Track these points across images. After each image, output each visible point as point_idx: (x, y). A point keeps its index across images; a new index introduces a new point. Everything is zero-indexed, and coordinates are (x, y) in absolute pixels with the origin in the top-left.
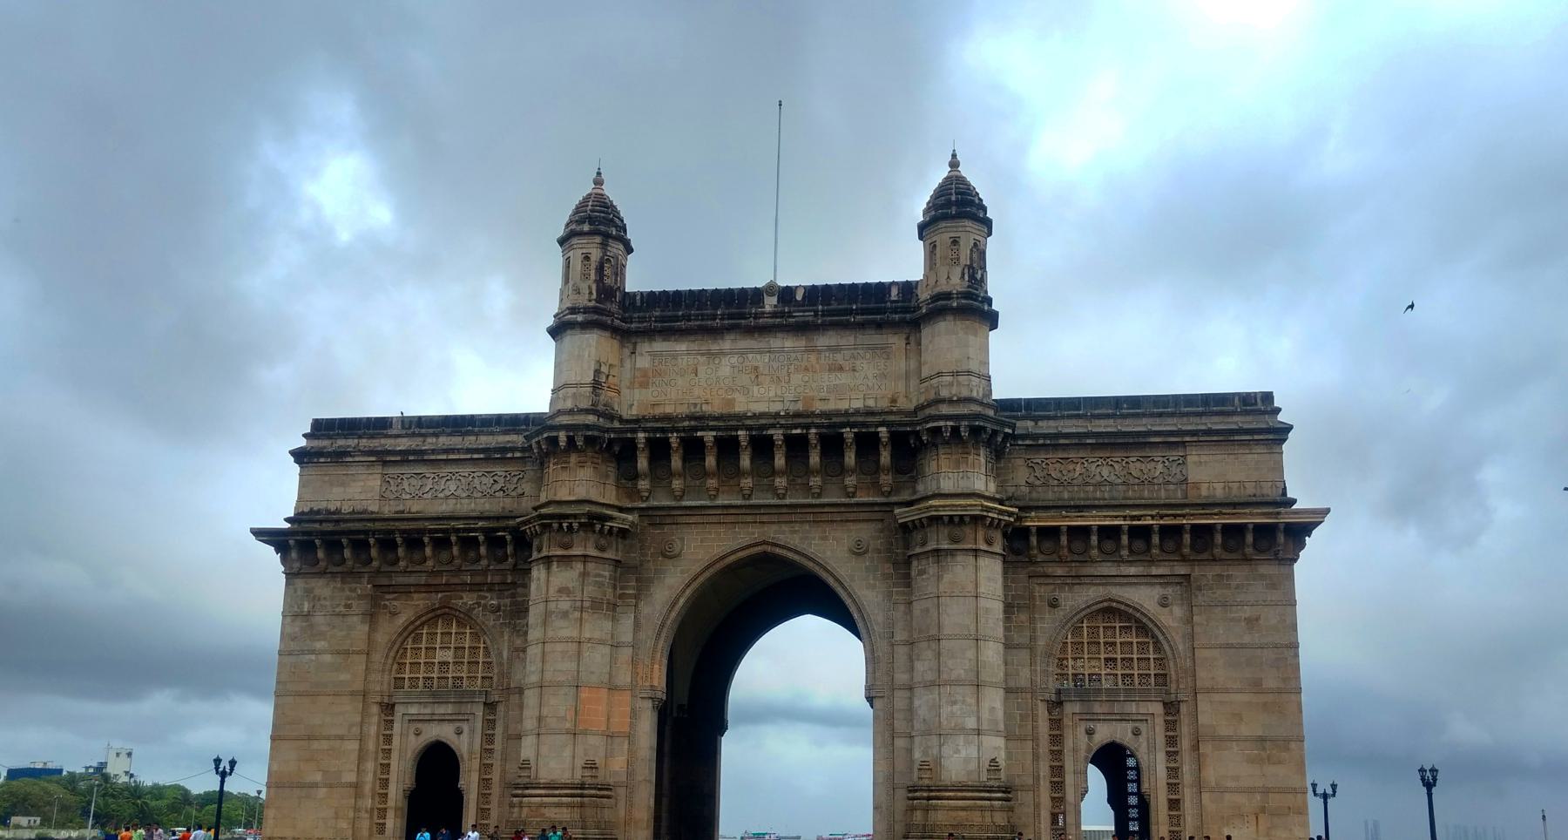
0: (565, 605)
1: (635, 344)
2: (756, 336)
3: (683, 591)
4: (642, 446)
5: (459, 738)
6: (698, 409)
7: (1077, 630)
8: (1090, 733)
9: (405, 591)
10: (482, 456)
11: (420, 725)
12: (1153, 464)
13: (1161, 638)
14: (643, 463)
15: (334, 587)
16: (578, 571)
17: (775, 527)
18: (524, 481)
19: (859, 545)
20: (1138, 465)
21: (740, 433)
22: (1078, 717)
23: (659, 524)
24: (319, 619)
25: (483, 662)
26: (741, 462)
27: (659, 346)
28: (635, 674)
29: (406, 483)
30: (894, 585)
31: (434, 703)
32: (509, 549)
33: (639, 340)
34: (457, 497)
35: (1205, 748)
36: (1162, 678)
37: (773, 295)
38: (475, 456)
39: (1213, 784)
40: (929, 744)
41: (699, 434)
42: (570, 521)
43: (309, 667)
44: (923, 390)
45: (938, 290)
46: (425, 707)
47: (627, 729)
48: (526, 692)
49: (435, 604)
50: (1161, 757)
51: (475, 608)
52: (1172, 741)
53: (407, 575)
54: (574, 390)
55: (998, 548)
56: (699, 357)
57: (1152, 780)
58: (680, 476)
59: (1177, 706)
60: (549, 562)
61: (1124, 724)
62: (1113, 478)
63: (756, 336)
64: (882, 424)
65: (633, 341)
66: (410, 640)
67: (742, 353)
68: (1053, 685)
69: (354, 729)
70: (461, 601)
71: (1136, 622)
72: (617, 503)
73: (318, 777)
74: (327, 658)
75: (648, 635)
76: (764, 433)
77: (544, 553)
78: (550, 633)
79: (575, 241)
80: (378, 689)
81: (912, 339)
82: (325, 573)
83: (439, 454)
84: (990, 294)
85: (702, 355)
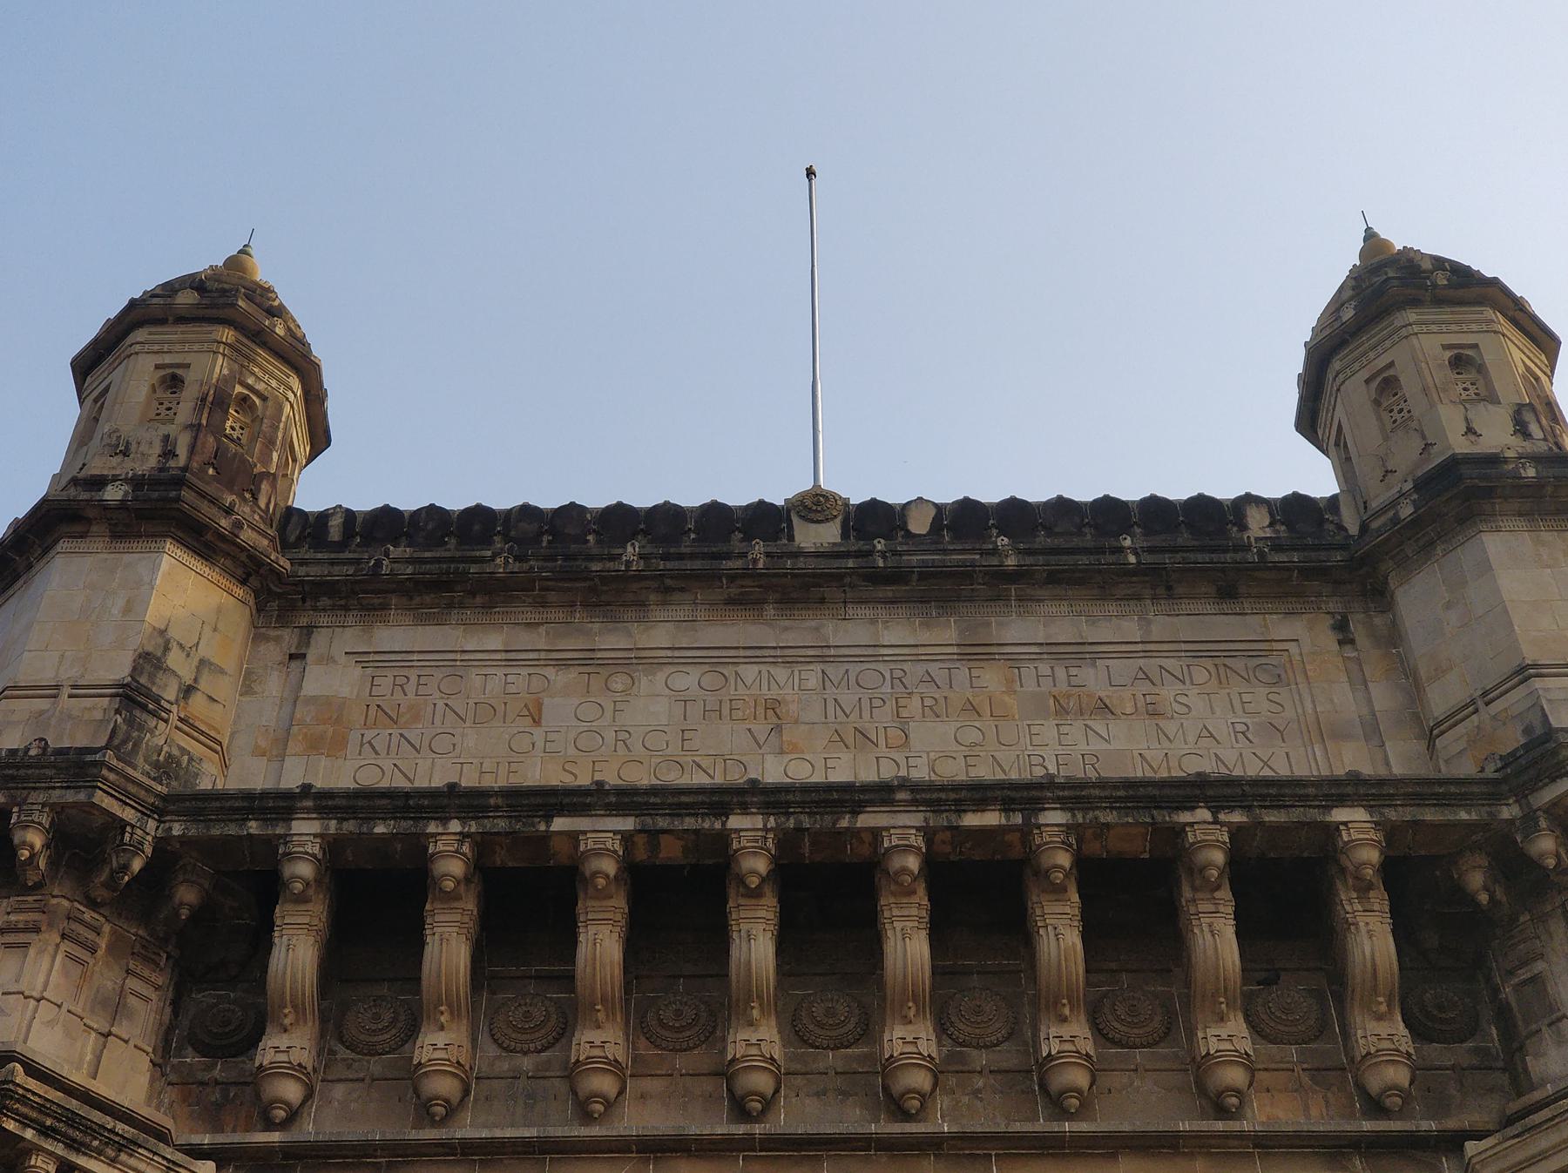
1: (309, 630)
2: (770, 611)
4: (305, 869)
21: (735, 822)
26: (737, 952)
33: (324, 620)
54: (43, 704)
56: (550, 672)
58: (455, 1014)
63: (770, 611)
64: (1342, 801)
65: (304, 621)
67: (717, 660)
72: (146, 1112)
76: (844, 823)
79: (140, 335)
81: (1357, 629)
85: (562, 664)
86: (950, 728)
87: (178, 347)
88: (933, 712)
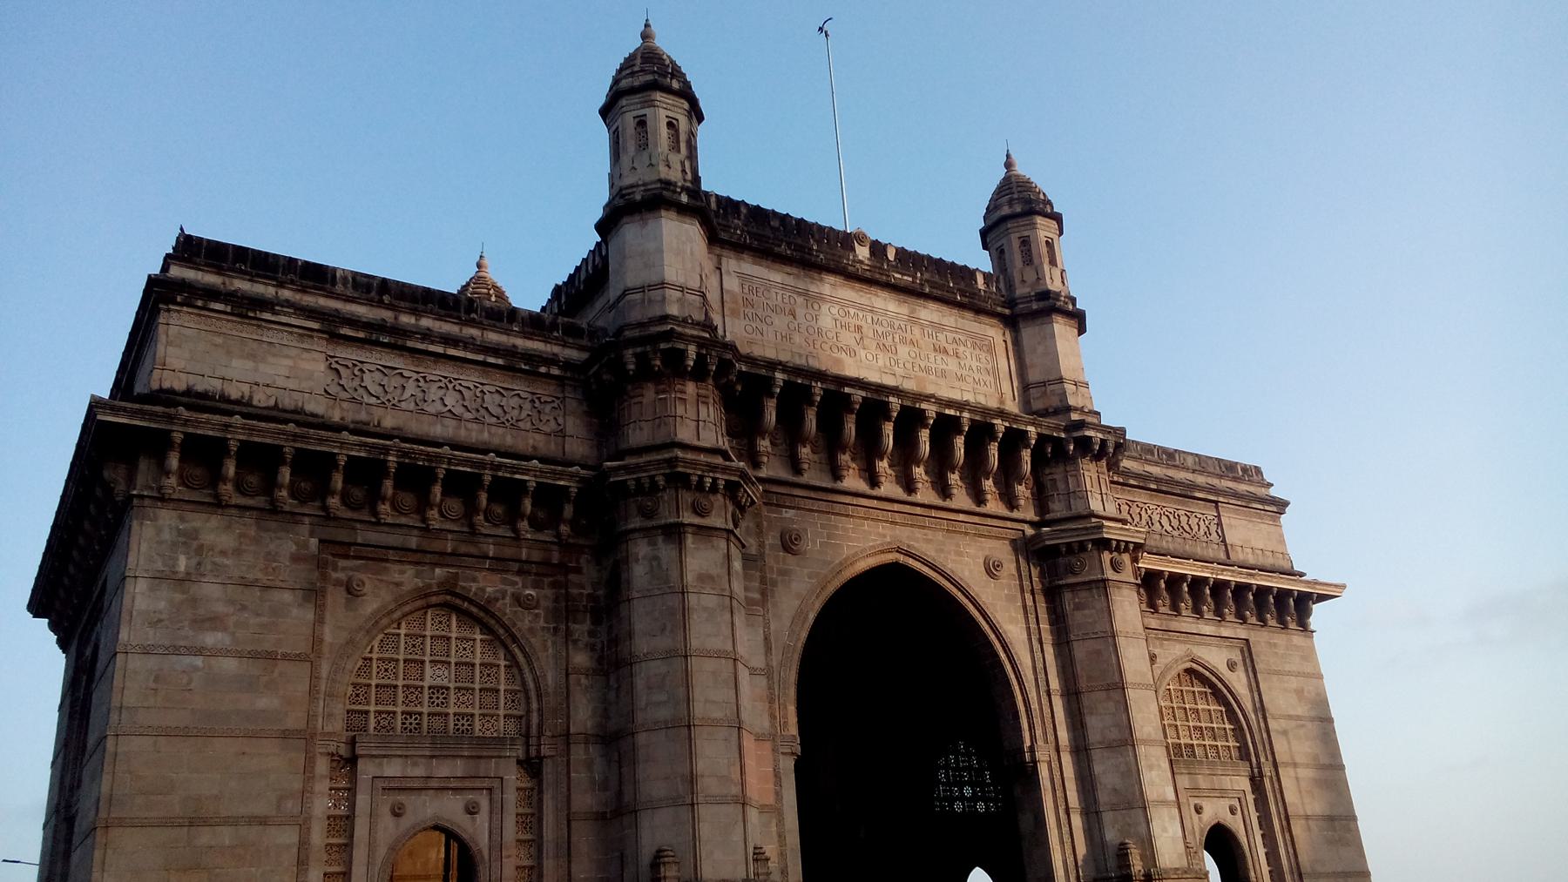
0: (710, 601)
1: (719, 257)
5: (474, 820)
8: (1198, 810)
9: (377, 556)
10: (500, 362)
11: (402, 798)
14: (771, 416)
15: (241, 535)
16: (721, 552)
18: (558, 411)
19: (998, 566)
21: (892, 399)
23: (778, 505)
24: (210, 589)
25: (505, 691)
27: (750, 267)
28: (773, 716)
29: (368, 380)
31: (432, 757)
33: (725, 253)
34: (458, 418)
37: (861, 243)
38: (491, 360)
39: (1309, 870)
40: (1128, 819)
41: (847, 390)
42: (718, 475)
43: (188, 684)
44: (1036, 396)
45: (1040, 289)
46: (415, 764)
47: (771, 800)
48: (642, 738)
49: (430, 586)
51: (497, 600)
53: (386, 529)
54: (679, 294)
56: (795, 296)
57: (1257, 867)
59: (1258, 782)
60: (680, 534)
62: (1170, 529)
66: (376, 643)
69: (289, 804)
70: (474, 586)
71: (1209, 688)
74: (229, 665)
78: (695, 643)
80: (328, 729)
83: (432, 343)
85: (799, 294)
86: (907, 350)
87: (672, 108)
88: (903, 341)
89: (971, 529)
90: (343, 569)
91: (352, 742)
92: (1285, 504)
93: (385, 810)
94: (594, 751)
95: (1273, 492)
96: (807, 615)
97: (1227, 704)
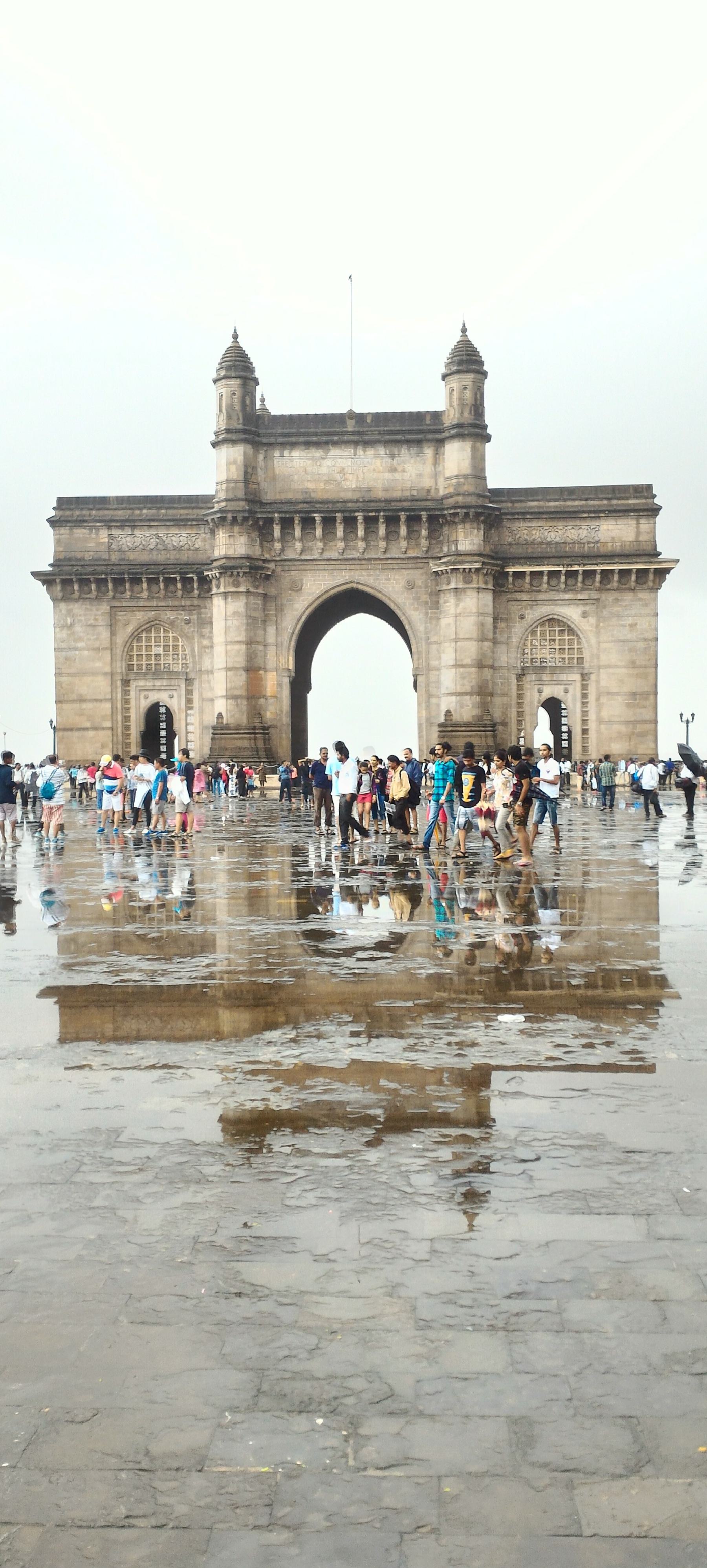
3: (304, 612)
6: (308, 496)
7: (533, 633)
8: (540, 692)
11: (146, 693)
12: (581, 531)
13: (581, 636)
15: (86, 609)
17: (357, 573)
20: (572, 531)
22: (533, 683)
24: (78, 629)
30: (431, 608)
32: (196, 585)
34: (158, 550)
35: (603, 700)
36: (581, 660)
37: (352, 419)
50: (579, 705)
52: (584, 696)
54: (232, 485)
55: (490, 586)
61: (559, 686)
67: (335, 458)
68: (519, 666)
73: (88, 725)
75: (285, 637)
77: (222, 589)
82: (80, 598)
84: (486, 422)
89: (396, 567)
90: (121, 616)
91: (127, 675)
92: (660, 508)
93: (142, 696)
94: (211, 676)
95: (656, 501)
96: (301, 617)
97: (577, 635)
